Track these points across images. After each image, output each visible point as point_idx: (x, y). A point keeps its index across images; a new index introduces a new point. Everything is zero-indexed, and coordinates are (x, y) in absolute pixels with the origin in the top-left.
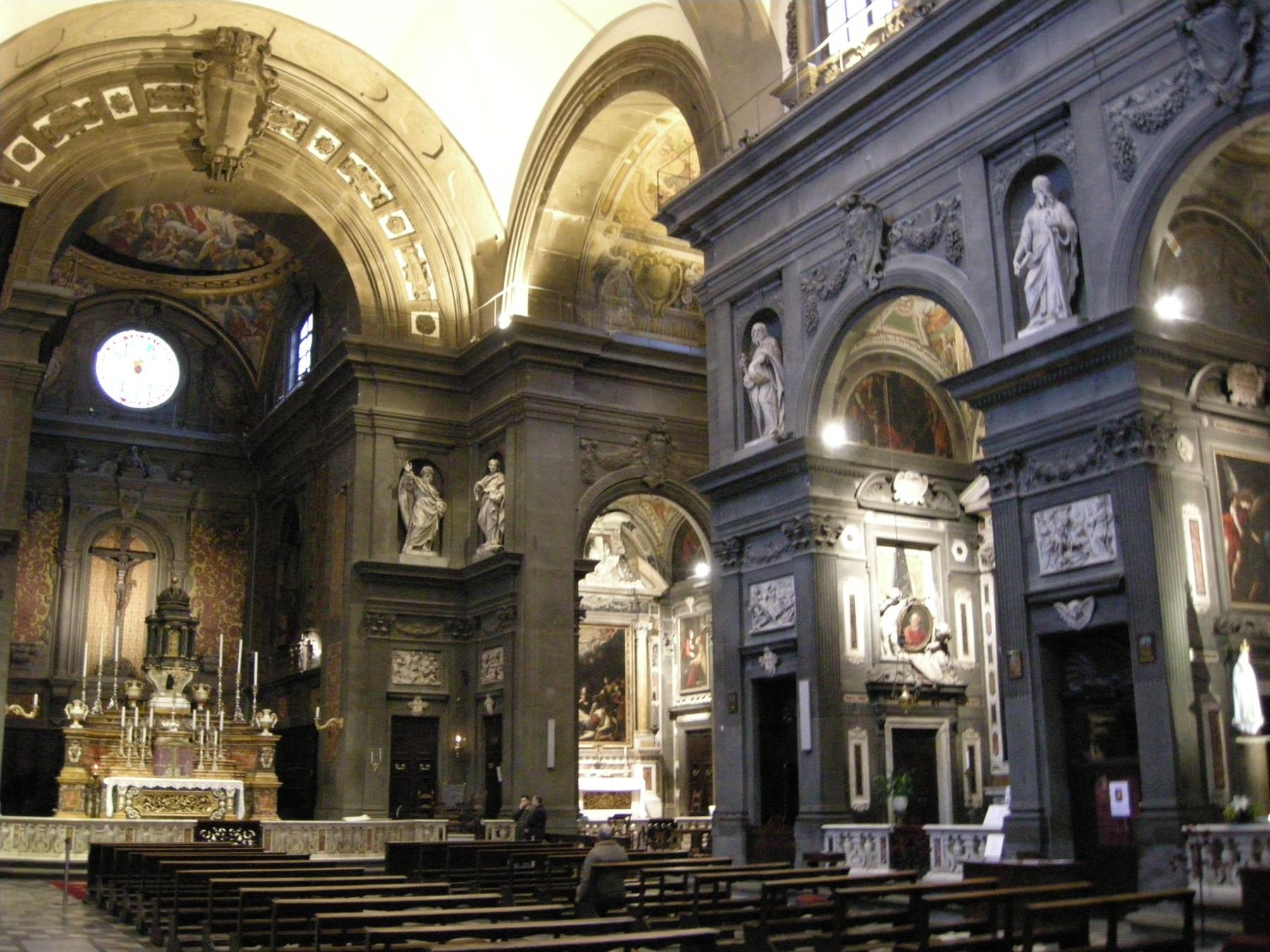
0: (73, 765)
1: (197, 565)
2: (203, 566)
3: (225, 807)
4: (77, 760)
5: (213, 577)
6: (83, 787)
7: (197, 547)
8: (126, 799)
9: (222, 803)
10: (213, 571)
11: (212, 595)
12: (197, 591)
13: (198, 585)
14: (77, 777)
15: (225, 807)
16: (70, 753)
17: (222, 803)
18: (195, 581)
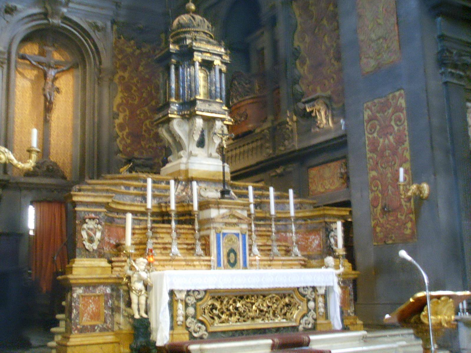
0: (89, 254)
1: (121, 73)
2: (126, 75)
3: (315, 310)
4: (95, 246)
5: (136, 86)
6: (108, 290)
7: (120, 57)
8: (187, 305)
9: (311, 304)
10: (135, 80)
11: (136, 102)
12: (121, 98)
13: (122, 91)
14: (98, 274)
15: (315, 310)
16: (84, 234)
17: (311, 304)
18: (120, 89)
